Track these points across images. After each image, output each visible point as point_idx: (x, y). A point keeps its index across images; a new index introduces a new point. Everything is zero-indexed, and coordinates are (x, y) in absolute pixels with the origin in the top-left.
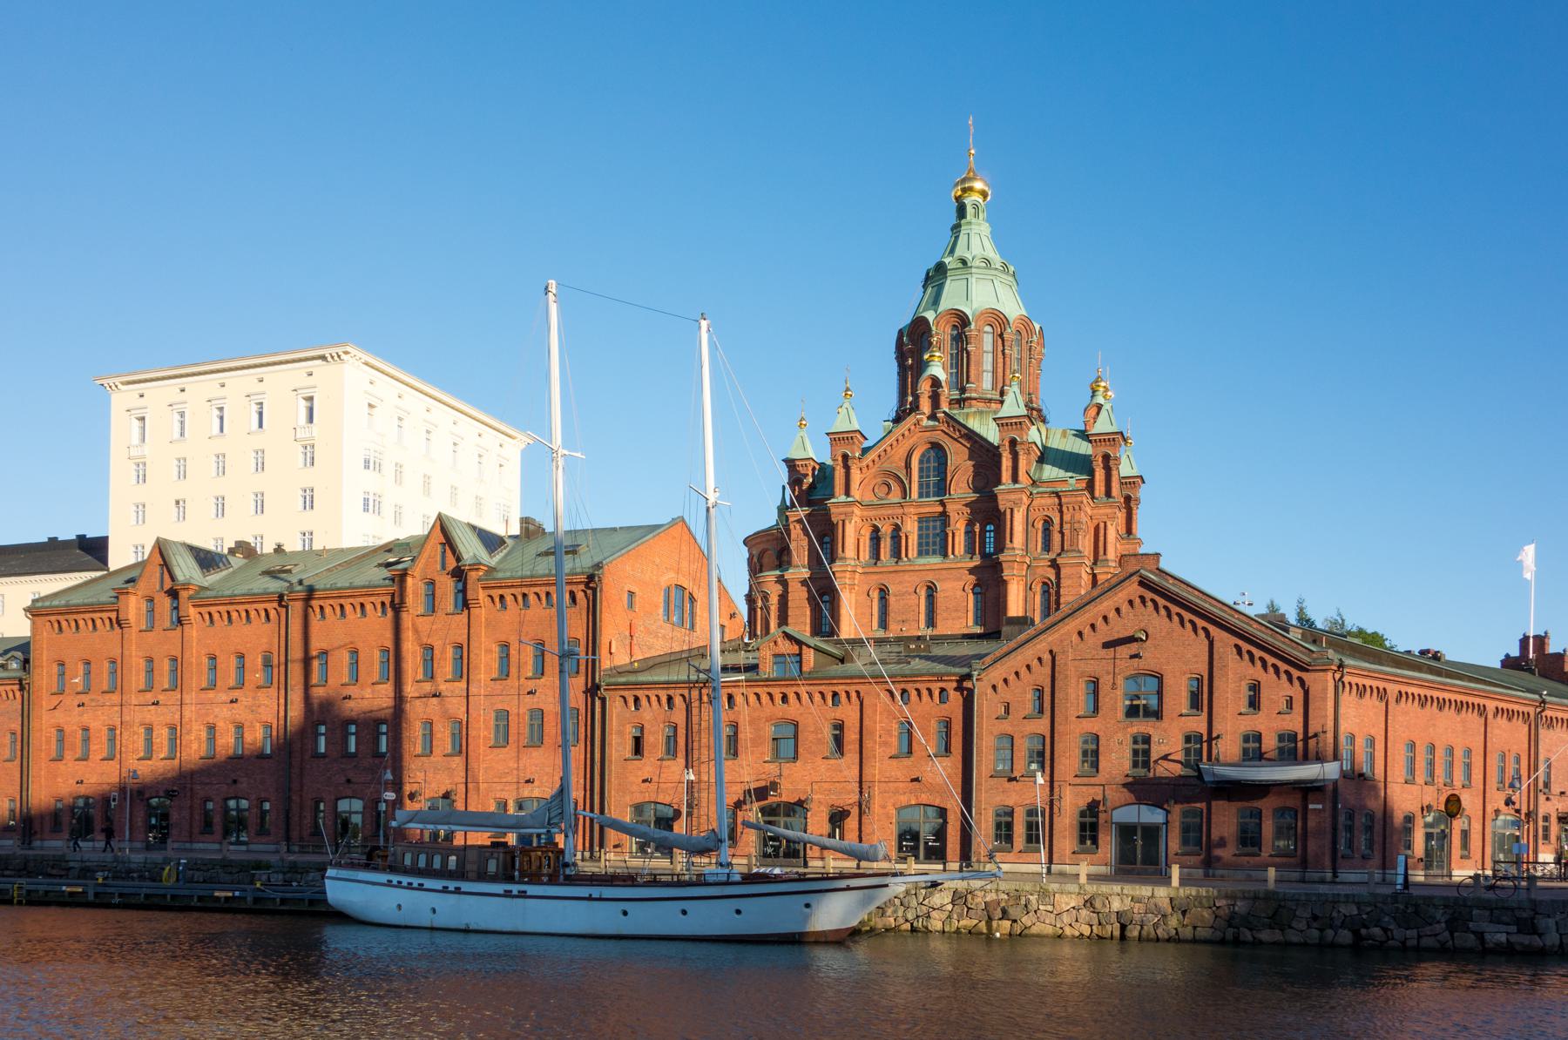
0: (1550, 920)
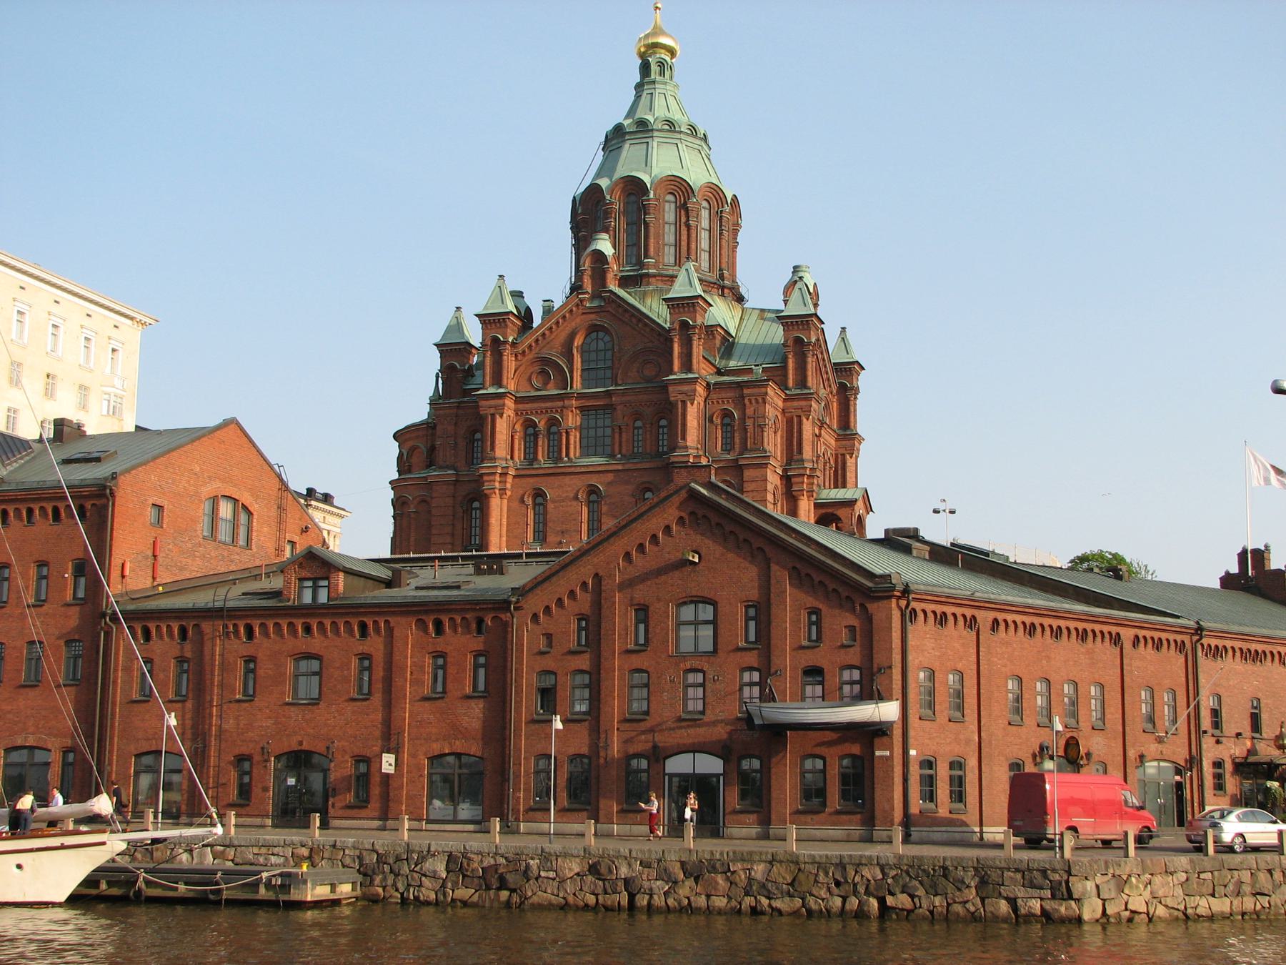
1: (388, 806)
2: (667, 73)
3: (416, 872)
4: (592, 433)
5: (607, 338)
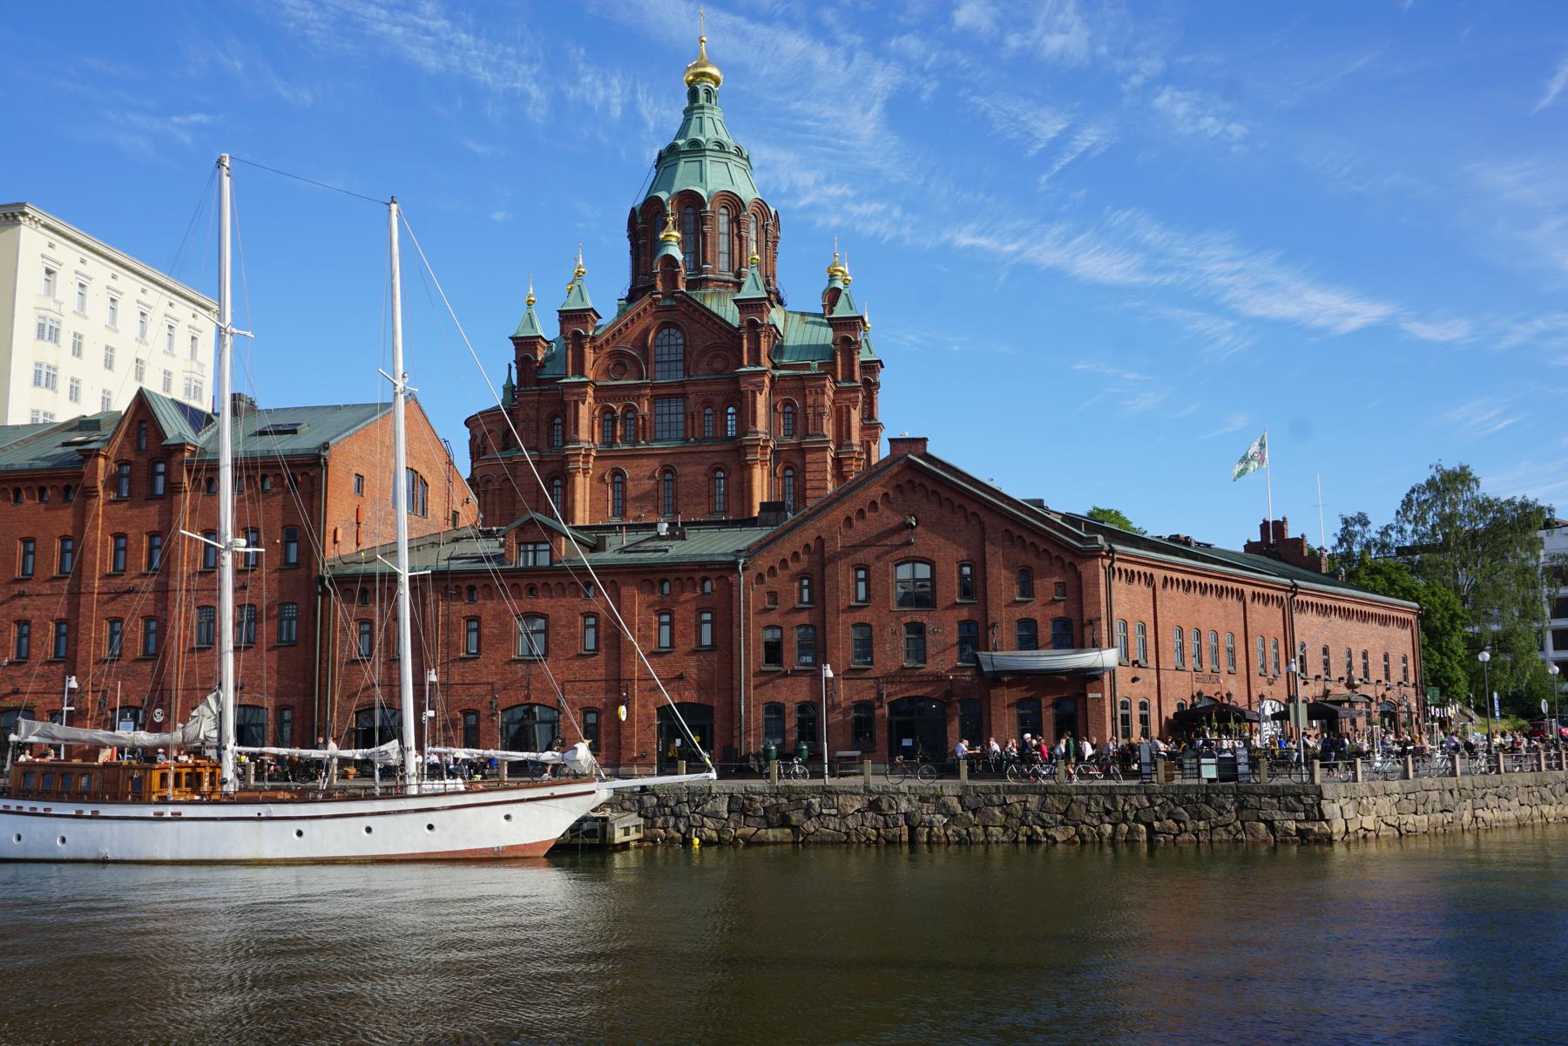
0: (1335, 805)
1: (620, 754)
2: (713, 100)
4: (666, 418)
5: (678, 334)
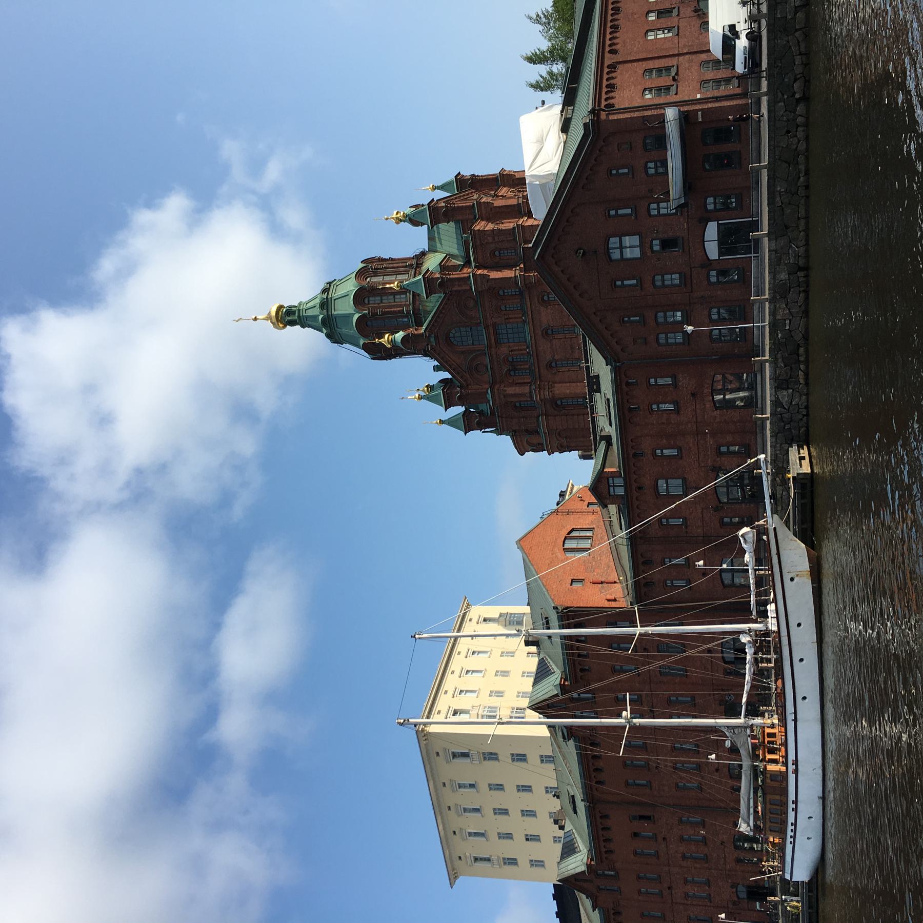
3: (789, 408)
4: (510, 336)
5: (453, 331)
